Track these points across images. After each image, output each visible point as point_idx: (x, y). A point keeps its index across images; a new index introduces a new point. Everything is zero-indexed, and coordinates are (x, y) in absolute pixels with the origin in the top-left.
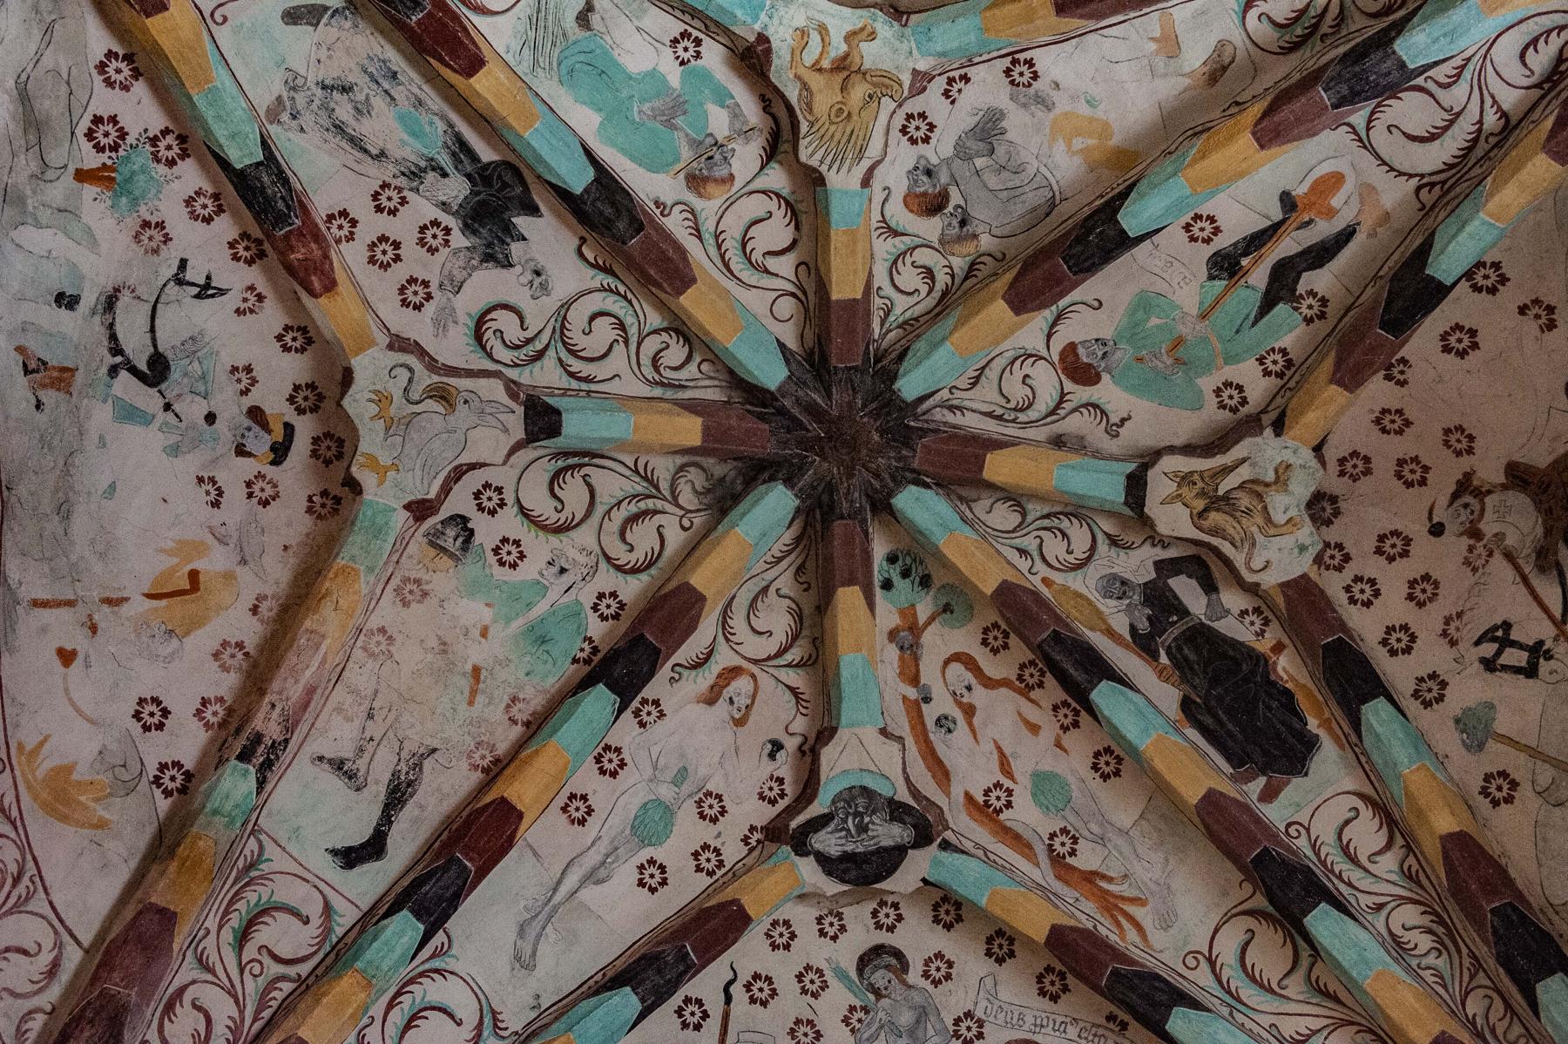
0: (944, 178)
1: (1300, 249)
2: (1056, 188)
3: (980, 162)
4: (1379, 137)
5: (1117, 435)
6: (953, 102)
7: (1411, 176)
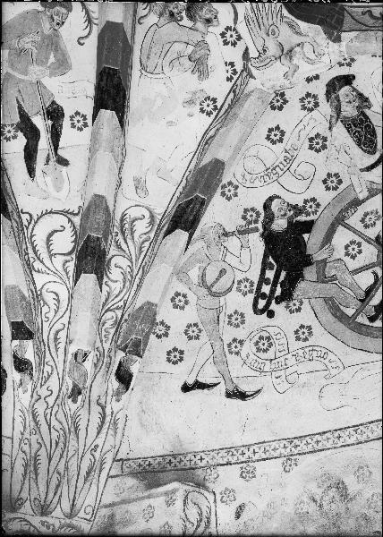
0: (200, 25)
1: (39, 148)
2: (149, 75)
3: (191, 48)
4: (63, 220)
6: (226, 63)
7: (38, 219)
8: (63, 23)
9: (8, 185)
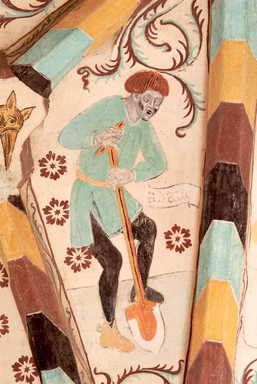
5: (79, 72)
8: (156, 111)
9: (75, 333)
